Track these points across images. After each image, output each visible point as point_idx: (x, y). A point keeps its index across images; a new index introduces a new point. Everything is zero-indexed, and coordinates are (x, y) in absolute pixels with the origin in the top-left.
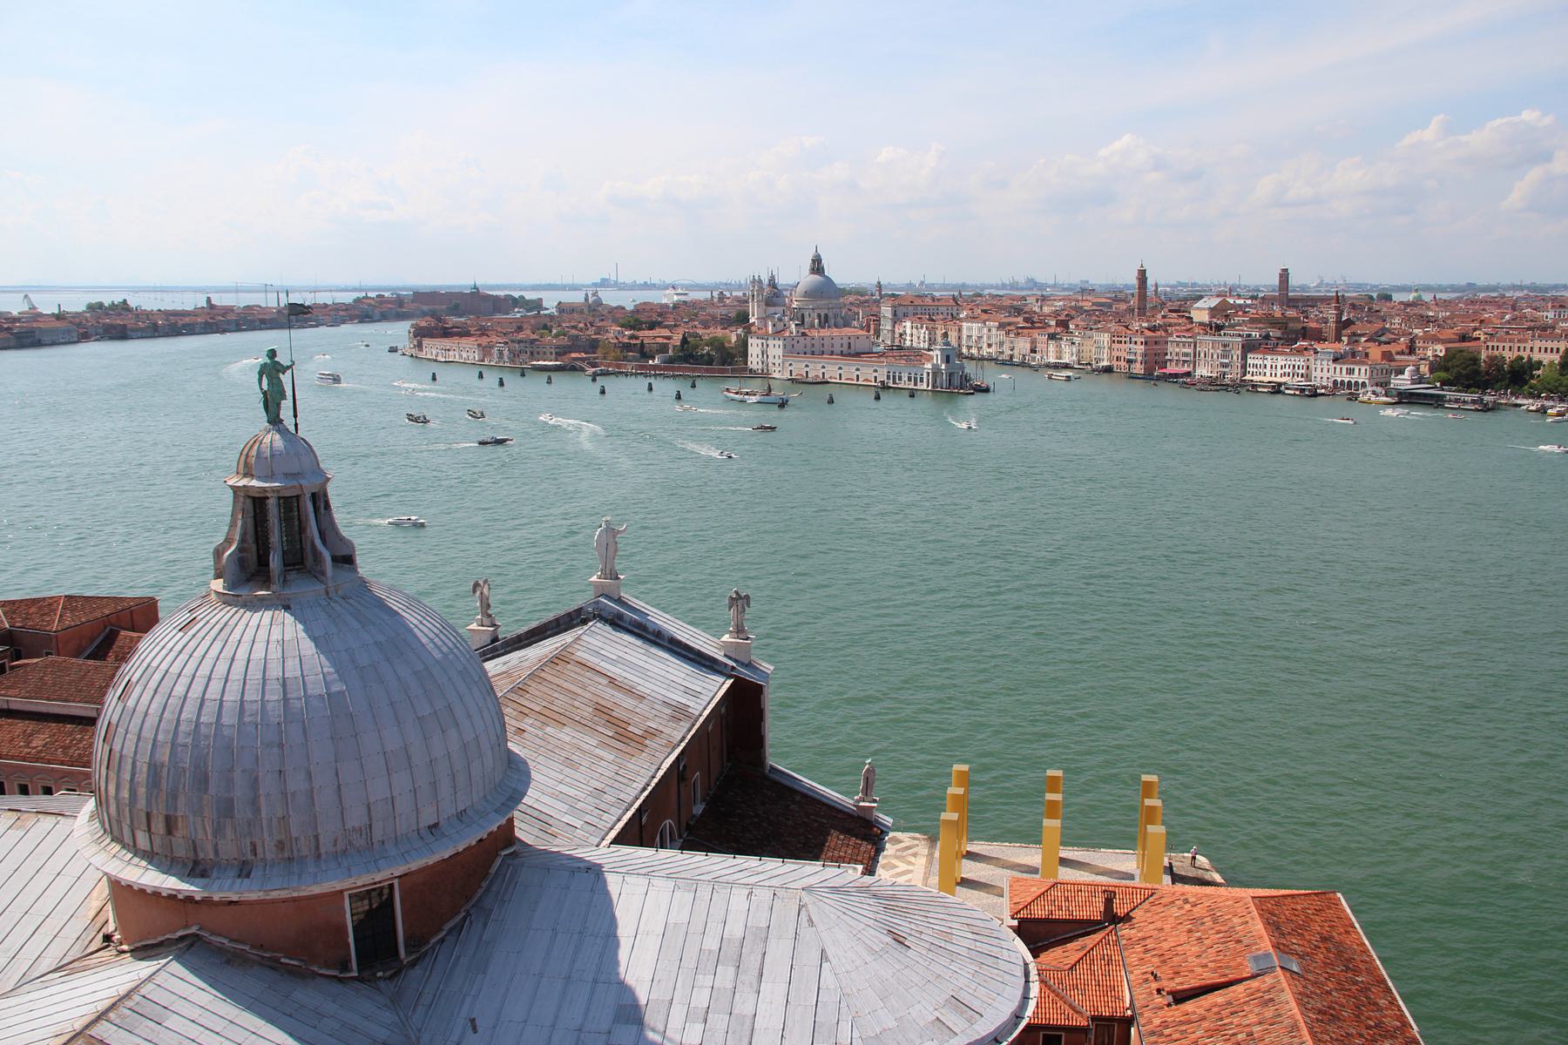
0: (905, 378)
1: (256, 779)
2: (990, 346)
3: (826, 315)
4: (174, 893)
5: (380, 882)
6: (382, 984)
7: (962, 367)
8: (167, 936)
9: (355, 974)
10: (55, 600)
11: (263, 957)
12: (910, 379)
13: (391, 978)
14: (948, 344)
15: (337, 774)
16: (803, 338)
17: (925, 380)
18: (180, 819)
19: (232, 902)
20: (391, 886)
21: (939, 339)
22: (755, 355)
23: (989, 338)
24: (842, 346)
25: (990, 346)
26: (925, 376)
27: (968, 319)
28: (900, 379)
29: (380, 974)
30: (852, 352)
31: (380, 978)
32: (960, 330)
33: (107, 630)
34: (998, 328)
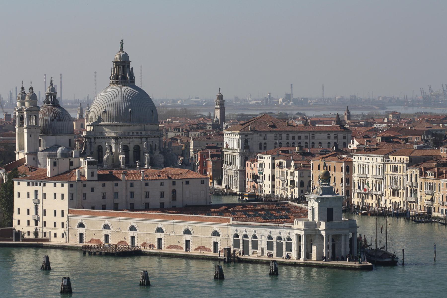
0: (263, 244)
2: (395, 192)
3: (137, 149)
7: (353, 226)
12: (270, 246)
14: (330, 191)
16: (100, 183)
17: (294, 247)
21: (316, 183)
22: (24, 211)
23: (394, 180)
24: (162, 195)
25: (395, 192)
26: (294, 242)
27: (359, 150)
28: (255, 245)
30: (178, 203)
32: (348, 169)
34: (409, 165)
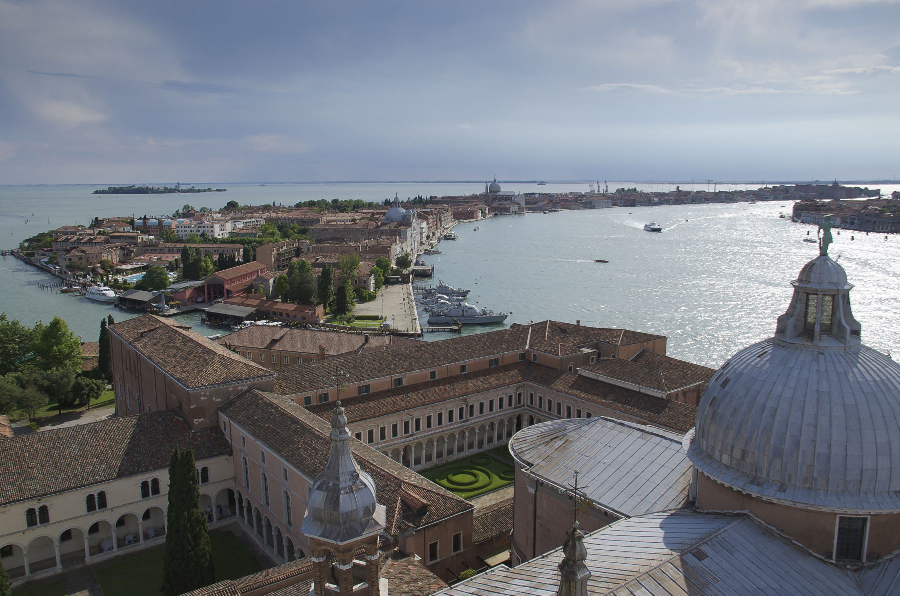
1: (799, 442)
4: (741, 490)
5: (860, 515)
6: (850, 573)
8: (730, 511)
9: (835, 562)
10: (618, 331)
11: (782, 537)
13: (855, 571)
15: (846, 449)
18: (751, 453)
19: (773, 503)
20: (865, 520)
29: (849, 567)
31: (848, 569)
33: (642, 349)
